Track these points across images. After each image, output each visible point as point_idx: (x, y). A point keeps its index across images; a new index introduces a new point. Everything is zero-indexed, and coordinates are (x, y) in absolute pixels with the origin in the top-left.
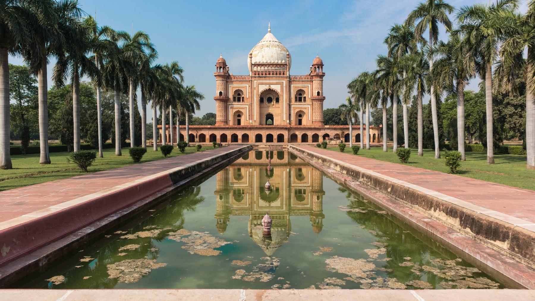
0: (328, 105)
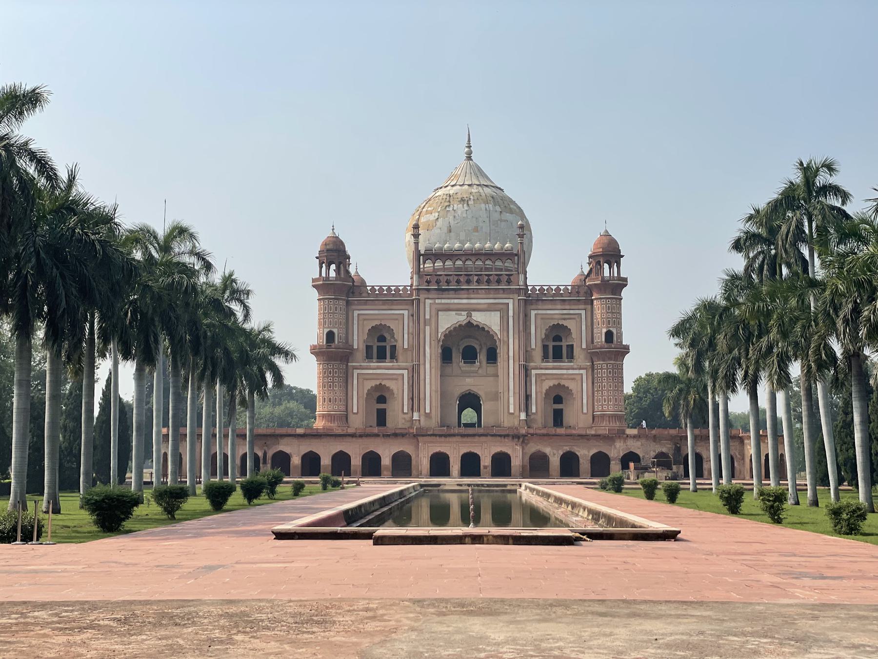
0: (633, 370)
